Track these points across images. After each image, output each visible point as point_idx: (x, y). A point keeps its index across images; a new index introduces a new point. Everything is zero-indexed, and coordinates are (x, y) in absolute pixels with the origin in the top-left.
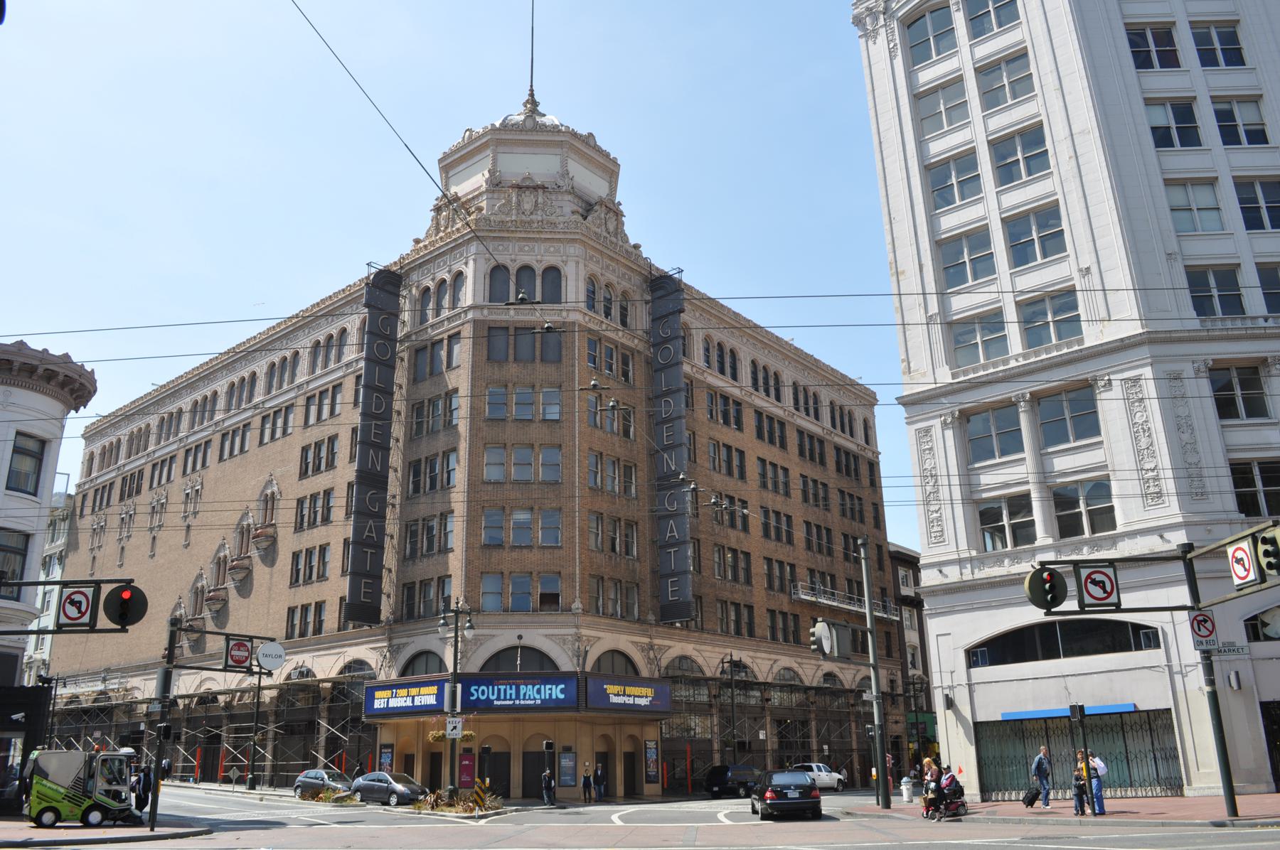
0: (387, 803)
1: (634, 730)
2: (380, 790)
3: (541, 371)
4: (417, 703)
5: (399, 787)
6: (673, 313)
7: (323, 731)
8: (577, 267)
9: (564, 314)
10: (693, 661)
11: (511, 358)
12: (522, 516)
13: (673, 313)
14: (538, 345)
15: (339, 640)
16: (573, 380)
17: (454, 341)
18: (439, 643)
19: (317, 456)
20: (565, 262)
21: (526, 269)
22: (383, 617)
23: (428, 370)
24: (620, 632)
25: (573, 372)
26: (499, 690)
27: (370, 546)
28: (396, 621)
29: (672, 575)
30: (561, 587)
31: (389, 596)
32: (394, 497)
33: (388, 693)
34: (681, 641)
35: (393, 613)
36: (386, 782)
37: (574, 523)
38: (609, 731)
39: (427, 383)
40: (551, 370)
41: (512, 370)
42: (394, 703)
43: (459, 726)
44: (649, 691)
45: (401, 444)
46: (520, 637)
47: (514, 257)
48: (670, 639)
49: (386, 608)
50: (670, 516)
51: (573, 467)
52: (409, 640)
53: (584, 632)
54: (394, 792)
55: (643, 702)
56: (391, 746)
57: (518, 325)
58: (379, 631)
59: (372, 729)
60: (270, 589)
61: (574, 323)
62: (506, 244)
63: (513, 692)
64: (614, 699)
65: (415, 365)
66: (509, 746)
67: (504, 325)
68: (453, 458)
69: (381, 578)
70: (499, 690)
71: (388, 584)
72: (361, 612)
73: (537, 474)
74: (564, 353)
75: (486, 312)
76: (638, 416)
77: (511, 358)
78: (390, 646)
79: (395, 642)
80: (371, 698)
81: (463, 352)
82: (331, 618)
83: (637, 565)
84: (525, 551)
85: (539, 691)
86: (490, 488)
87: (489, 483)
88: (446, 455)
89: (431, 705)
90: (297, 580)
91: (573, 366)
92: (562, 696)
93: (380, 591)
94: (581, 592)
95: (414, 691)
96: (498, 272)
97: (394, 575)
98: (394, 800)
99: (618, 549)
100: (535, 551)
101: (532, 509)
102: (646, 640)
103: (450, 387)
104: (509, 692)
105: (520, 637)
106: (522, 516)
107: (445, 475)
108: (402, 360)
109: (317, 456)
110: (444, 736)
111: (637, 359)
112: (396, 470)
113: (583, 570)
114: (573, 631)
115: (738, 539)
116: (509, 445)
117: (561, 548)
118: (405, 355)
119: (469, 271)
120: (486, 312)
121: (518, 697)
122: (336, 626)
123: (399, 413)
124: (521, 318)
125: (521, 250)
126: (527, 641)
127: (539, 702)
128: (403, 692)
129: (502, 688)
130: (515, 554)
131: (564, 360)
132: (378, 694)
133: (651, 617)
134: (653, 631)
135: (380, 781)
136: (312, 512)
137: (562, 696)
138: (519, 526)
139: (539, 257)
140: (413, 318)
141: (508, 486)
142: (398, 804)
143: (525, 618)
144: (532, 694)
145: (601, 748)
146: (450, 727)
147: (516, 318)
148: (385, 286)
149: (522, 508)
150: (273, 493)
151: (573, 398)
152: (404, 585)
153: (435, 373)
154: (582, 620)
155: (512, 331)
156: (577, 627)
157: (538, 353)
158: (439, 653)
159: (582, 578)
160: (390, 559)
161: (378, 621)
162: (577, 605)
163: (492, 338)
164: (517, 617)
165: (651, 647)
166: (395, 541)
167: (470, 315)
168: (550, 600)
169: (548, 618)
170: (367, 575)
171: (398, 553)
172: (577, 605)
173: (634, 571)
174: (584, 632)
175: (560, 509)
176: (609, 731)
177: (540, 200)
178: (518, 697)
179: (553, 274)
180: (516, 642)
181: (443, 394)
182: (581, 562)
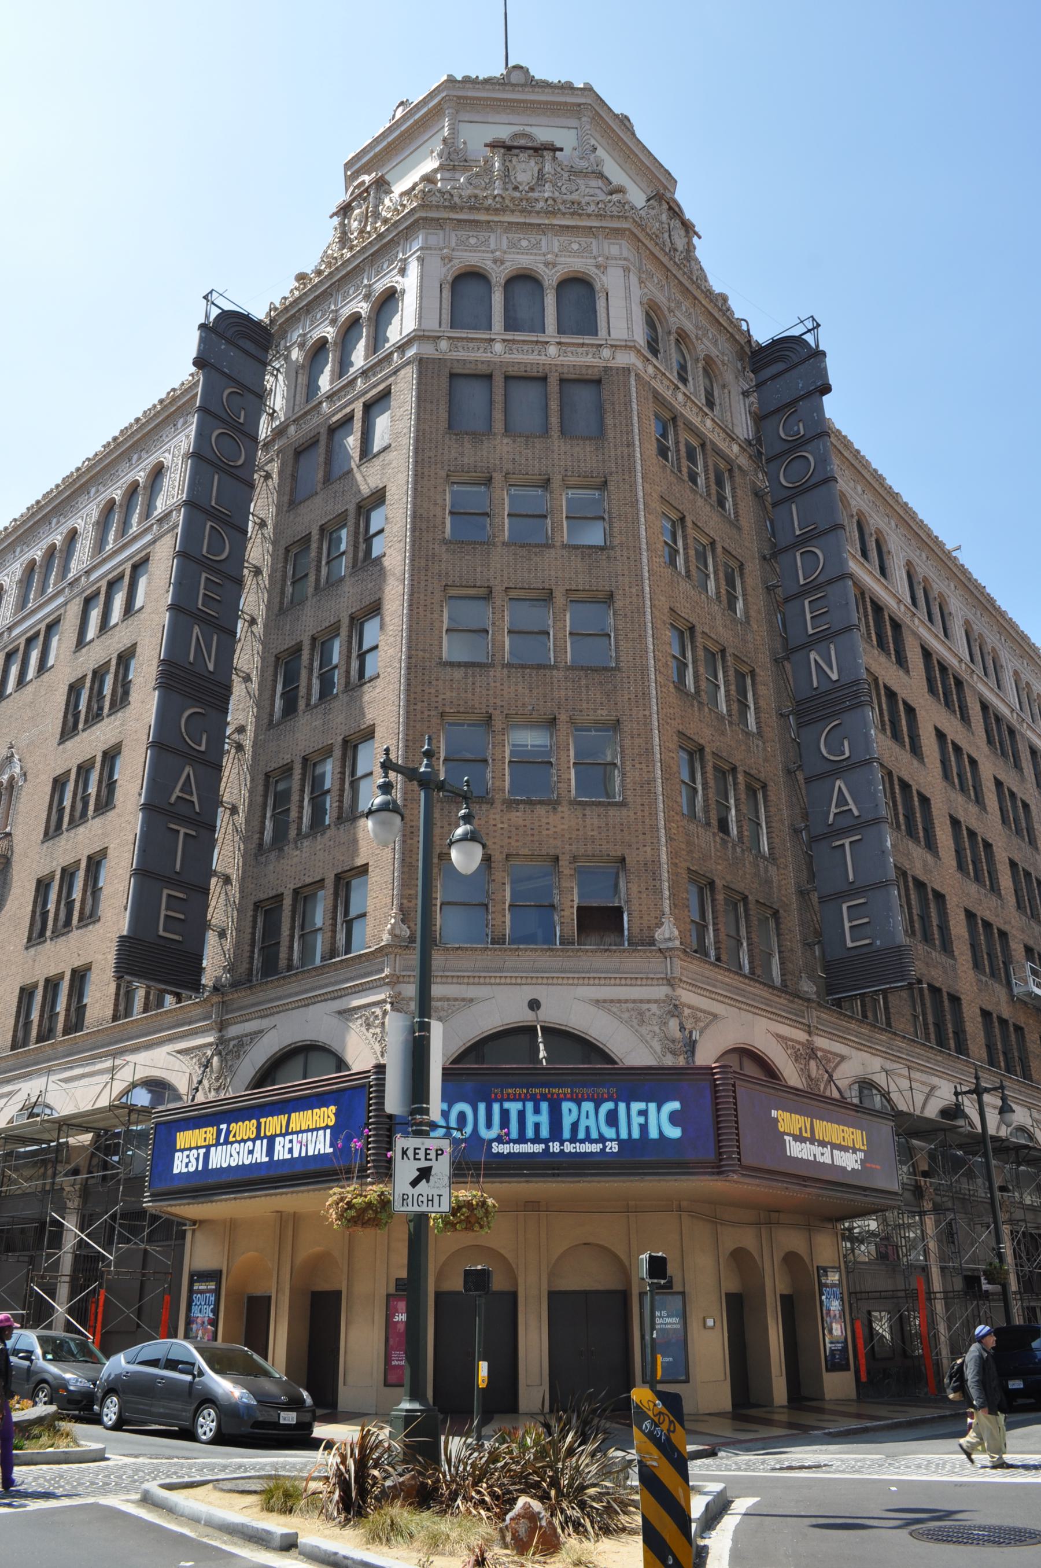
0: (189, 1434)
1: (792, 1240)
2: (172, 1390)
3: (562, 455)
4: (281, 1152)
5: (227, 1388)
6: (809, 394)
7: (69, 1243)
8: (627, 276)
9: (606, 353)
11: (499, 426)
12: (531, 739)
13: (809, 394)
14: (554, 406)
15: (118, 1040)
16: (632, 470)
17: (375, 410)
18: (335, 1021)
19: (97, 694)
20: (602, 268)
21: (524, 281)
22: (207, 980)
23: (320, 475)
24: (755, 1010)
25: (631, 456)
26: (505, 1114)
28: (235, 985)
29: (852, 891)
30: (631, 895)
31: (222, 934)
32: (241, 730)
33: (210, 1132)
34: (860, 1047)
35: (231, 968)
36: (189, 1367)
37: (649, 752)
38: (747, 1239)
39: (318, 500)
40: (582, 456)
41: (501, 450)
42: (220, 1158)
43: (442, 1168)
44: (855, 1136)
45: (259, 629)
46: (534, 1005)
47: (500, 254)
48: (843, 1040)
49: (214, 961)
50: (839, 770)
51: (642, 637)
52: (265, 1023)
53: (686, 996)
54: (208, 1400)
55: (849, 1161)
56: (214, 1276)
57: (512, 371)
58: (198, 1011)
59: (172, 1232)
61: (626, 371)
62: (483, 235)
63: (544, 1118)
64: (797, 1150)
65: (294, 477)
66: (512, 1275)
67: (483, 369)
68: (371, 628)
69: (206, 891)
70: (505, 1114)
71: (221, 908)
72: (159, 961)
73: (560, 649)
74: (609, 421)
75: (444, 345)
76: (749, 580)
77: (499, 426)
78: (221, 1041)
79: (233, 1031)
80: (166, 1150)
81: (393, 427)
82: (100, 996)
83: (773, 870)
84: (541, 810)
85: (612, 1119)
86: (458, 674)
87: (451, 664)
88: (357, 622)
89: (319, 1157)
90: (42, 933)
91: (630, 445)
92: (674, 1133)
93: (204, 925)
94: (674, 905)
95: (273, 1124)
96: (466, 284)
97: (234, 890)
98: (207, 1424)
100: (564, 809)
101: (552, 723)
102: (801, 1036)
103: (365, 490)
104: (531, 1119)
105: (534, 1005)
106: (531, 739)
107: (355, 664)
108: (268, 476)
109: (97, 694)
110: (385, 1203)
111: (738, 479)
112: (247, 679)
113: (673, 855)
114: (661, 991)
115: (925, 864)
116: (498, 589)
117: (623, 804)
118: (274, 468)
120: (444, 345)
121: (556, 1133)
122: (109, 1012)
123: (257, 572)
124: (517, 357)
125: (513, 245)
126: (552, 1014)
127: (613, 1147)
128: (245, 1128)
129: (514, 1107)
130: (517, 817)
131: (610, 434)
132: (184, 1138)
133: (808, 987)
134: (815, 1016)
135: (172, 1364)
136: (79, 796)
137: (674, 1133)
138: (523, 762)
139: (552, 257)
140: (291, 399)
141: (498, 672)
142: (220, 1439)
143: (544, 960)
144: (592, 1124)
145: (731, 1285)
146: (405, 1170)
147: (508, 357)
148: (234, 345)
149: (532, 724)
150: (12, 778)
151: (634, 504)
152: (257, 906)
153: (334, 475)
154: (678, 966)
155: (499, 381)
156: (670, 982)
157: (554, 420)
158: (335, 1046)
159: (674, 874)
160: (227, 855)
161: (196, 986)
162: (668, 932)
163: (455, 394)
164: (530, 957)
165: (812, 1052)
166: (241, 818)
167: (411, 352)
168: (601, 922)
169: (601, 961)
171: (245, 840)
172: (668, 932)
173: (768, 882)
174: (686, 996)
175: (616, 725)
176: (747, 1239)
177: (548, 168)
178: (556, 1133)
179: (579, 290)
180: (523, 1016)
181: (352, 508)
182: (670, 839)
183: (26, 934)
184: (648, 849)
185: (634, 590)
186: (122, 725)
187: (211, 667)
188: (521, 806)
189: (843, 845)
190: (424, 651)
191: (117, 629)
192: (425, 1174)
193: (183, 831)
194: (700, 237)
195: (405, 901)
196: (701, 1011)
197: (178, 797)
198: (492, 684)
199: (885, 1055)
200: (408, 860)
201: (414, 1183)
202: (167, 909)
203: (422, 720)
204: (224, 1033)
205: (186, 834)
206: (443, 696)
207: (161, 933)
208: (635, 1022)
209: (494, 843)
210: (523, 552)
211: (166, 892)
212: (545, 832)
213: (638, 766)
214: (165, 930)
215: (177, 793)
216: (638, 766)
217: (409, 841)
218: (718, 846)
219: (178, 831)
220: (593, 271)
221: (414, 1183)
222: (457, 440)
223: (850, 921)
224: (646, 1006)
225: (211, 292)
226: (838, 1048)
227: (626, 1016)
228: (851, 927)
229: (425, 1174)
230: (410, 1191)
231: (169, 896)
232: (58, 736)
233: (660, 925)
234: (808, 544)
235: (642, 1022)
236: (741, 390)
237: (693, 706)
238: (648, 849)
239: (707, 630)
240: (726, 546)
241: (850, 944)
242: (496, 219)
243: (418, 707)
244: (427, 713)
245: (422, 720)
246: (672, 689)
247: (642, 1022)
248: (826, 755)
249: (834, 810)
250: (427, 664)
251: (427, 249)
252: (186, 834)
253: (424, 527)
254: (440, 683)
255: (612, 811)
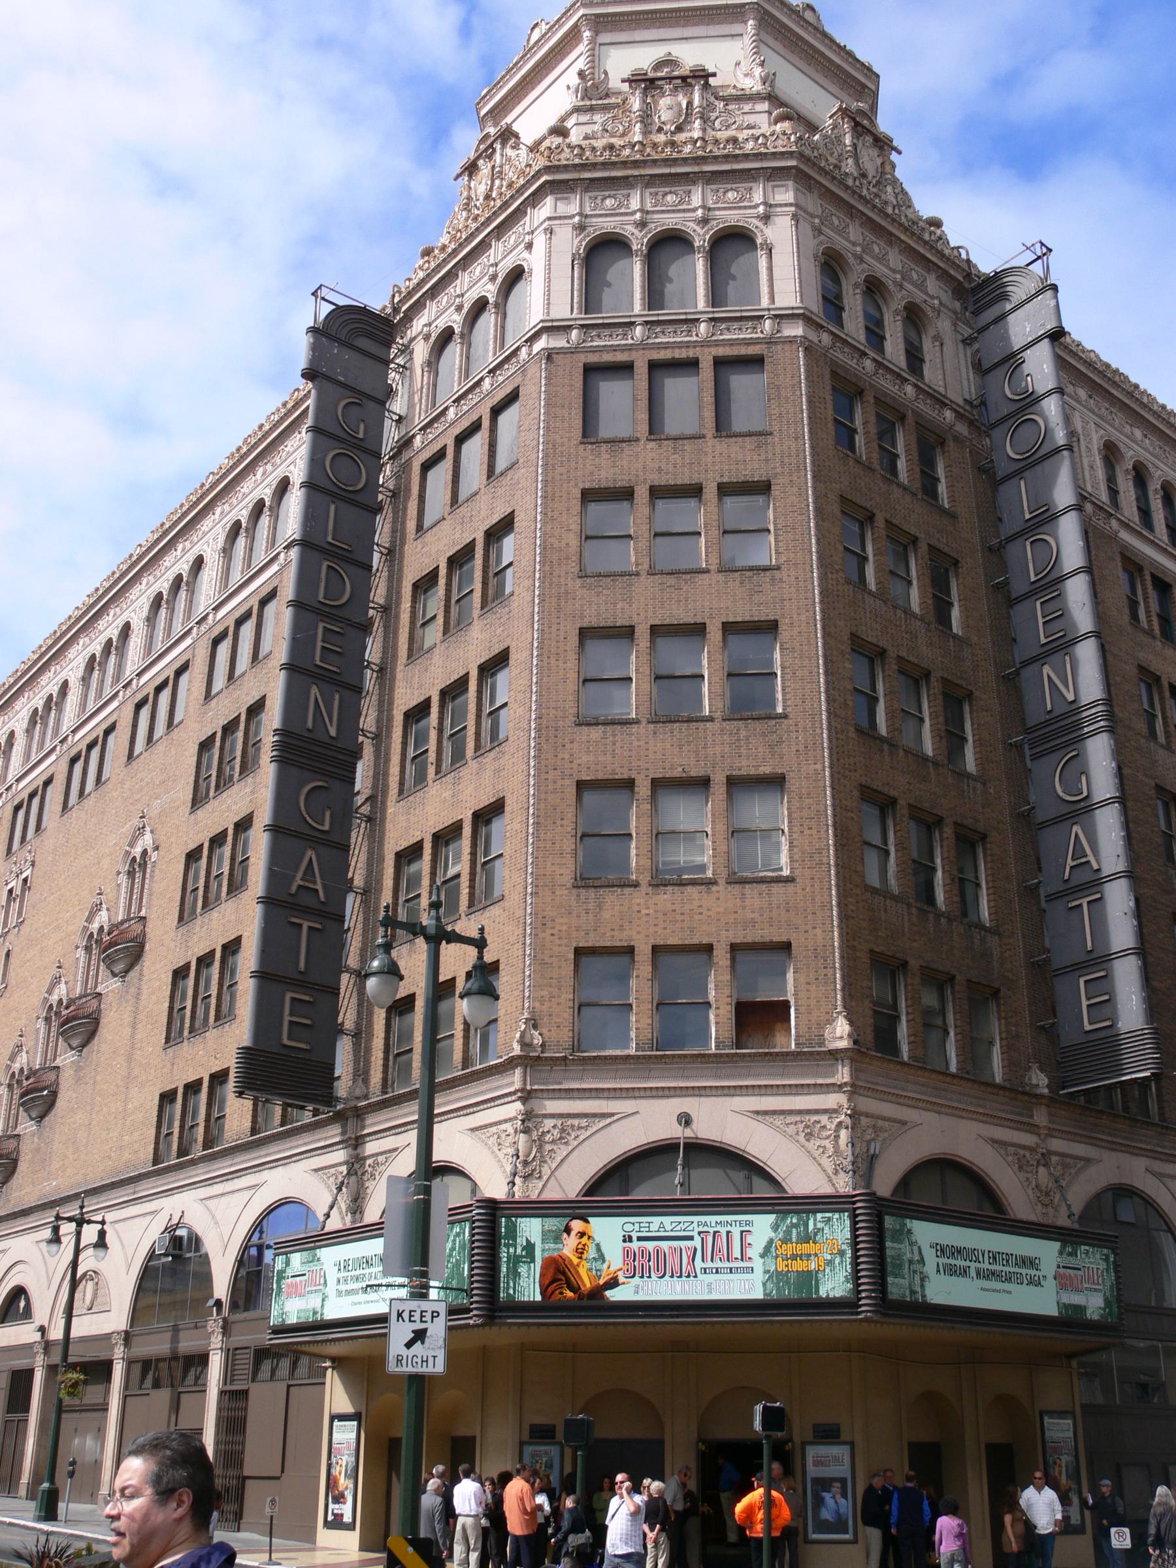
10: (1149, 1202)
24: (959, 1113)
27: (306, 911)
34: (1113, 1147)
60: (130, 1059)
69: (335, 991)
83: (993, 941)
99: (940, 896)
102: (1028, 1139)
105: (685, 1120)
119: (535, 261)
150: (145, 852)
170: (299, 982)
180: (676, 1132)
183: (164, 1034)
184: (818, 931)
185: (803, 618)
186: (253, 792)
187: (333, 732)
188: (670, 888)
189: (1080, 906)
190: (555, 708)
191: (246, 678)
192: (420, 1336)
193: (306, 925)
194: (899, 153)
195: (537, 1004)
196: (884, 1119)
197: (300, 886)
198: (636, 743)
199: (1153, 1155)
200: (540, 956)
201: (409, 1345)
202: (291, 1015)
203: (555, 791)
204: (359, 1151)
205: (310, 928)
206: (579, 762)
207: (286, 1041)
208: (801, 1137)
209: (638, 933)
210: (671, 580)
211: (289, 995)
212: (697, 917)
213: (807, 832)
214: (289, 1038)
215: (298, 881)
216: (807, 832)
217: (541, 935)
218: (914, 919)
219: (300, 926)
220: (754, 224)
221: (409, 1345)
222: (592, 450)
223: (1088, 999)
224: (814, 1118)
225: (320, 288)
226: (1079, 1149)
227: (791, 1130)
228: (1088, 1006)
229: (420, 1336)
230: (404, 1352)
231: (293, 999)
232: (190, 805)
233: (831, 1021)
234: (1040, 530)
235: (809, 1136)
236: (960, 337)
237: (882, 751)
238: (818, 931)
239: (903, 654)
240: (933, 542)
241: (1088, 1027)
242: (636, 172)
243: (550, 776)
244: (559, 782)
245: (555, 791)
246: (852, 734)
247: (809, 1136)
248: (1061, 794)
249: (1070, 863)
250: (561, 723)
251: (555, 218)
252: (310, 928)
253: (555, 557)
254: (575, 745)
255: (777, 888)
